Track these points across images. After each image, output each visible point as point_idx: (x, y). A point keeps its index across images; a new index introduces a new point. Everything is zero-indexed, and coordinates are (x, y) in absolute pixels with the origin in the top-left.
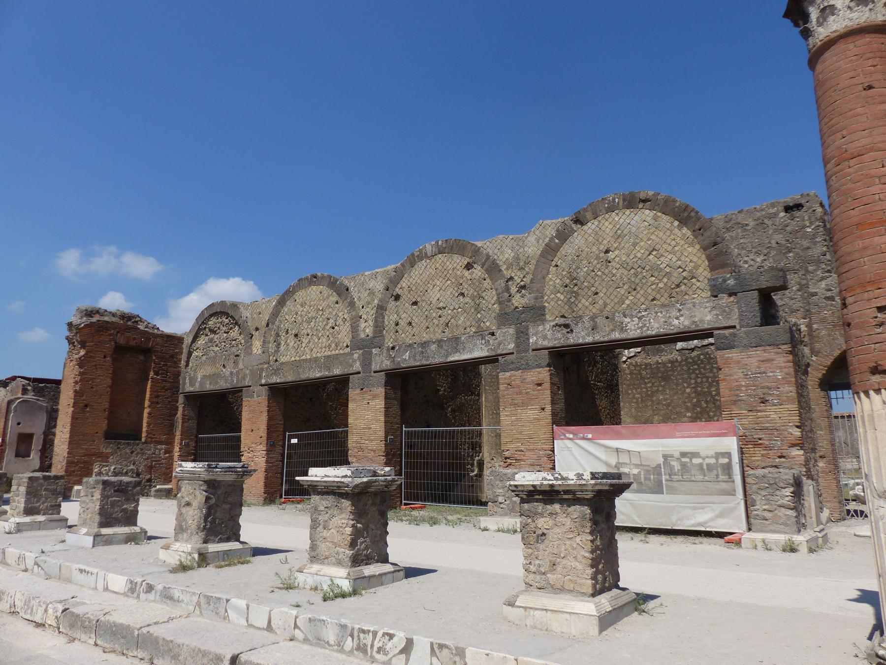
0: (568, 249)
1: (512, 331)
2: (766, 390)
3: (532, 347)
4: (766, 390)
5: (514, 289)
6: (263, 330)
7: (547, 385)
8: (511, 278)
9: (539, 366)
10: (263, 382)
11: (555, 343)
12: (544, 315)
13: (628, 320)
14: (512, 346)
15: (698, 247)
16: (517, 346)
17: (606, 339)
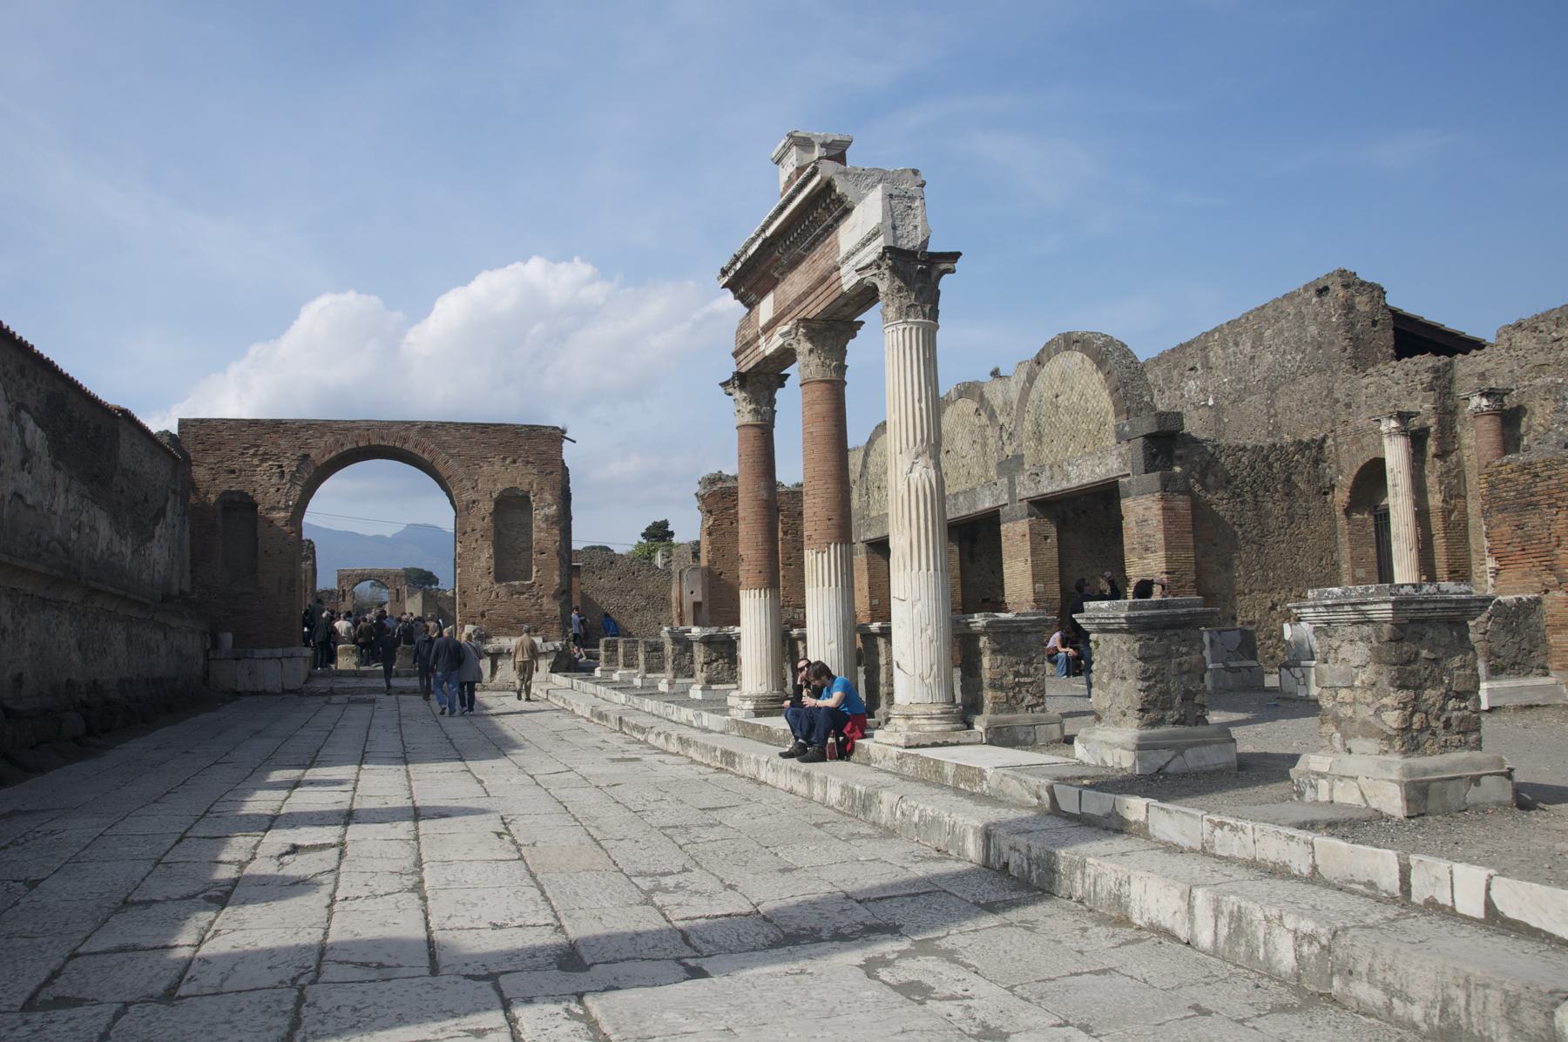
0: (1033, 395)
1: (1005, 480)
2: (1147, 538)
3: (1018, 498)
4: (1147, 538)
5: (1005, 437)
6: (858, 483)
7: (1028, 536)
8: (1003, 425)
9: (1023, 518)
10: (862, 538)
11: (1032, 494)
12: (1023, 464)
13: (1070, 468)
14: (1006, 497)
15: (1107, 391)
16: (1010, 497)
17: (1058, 489)
